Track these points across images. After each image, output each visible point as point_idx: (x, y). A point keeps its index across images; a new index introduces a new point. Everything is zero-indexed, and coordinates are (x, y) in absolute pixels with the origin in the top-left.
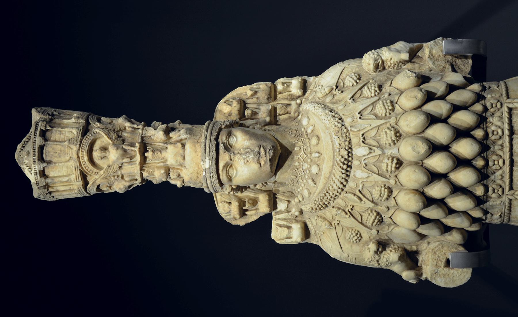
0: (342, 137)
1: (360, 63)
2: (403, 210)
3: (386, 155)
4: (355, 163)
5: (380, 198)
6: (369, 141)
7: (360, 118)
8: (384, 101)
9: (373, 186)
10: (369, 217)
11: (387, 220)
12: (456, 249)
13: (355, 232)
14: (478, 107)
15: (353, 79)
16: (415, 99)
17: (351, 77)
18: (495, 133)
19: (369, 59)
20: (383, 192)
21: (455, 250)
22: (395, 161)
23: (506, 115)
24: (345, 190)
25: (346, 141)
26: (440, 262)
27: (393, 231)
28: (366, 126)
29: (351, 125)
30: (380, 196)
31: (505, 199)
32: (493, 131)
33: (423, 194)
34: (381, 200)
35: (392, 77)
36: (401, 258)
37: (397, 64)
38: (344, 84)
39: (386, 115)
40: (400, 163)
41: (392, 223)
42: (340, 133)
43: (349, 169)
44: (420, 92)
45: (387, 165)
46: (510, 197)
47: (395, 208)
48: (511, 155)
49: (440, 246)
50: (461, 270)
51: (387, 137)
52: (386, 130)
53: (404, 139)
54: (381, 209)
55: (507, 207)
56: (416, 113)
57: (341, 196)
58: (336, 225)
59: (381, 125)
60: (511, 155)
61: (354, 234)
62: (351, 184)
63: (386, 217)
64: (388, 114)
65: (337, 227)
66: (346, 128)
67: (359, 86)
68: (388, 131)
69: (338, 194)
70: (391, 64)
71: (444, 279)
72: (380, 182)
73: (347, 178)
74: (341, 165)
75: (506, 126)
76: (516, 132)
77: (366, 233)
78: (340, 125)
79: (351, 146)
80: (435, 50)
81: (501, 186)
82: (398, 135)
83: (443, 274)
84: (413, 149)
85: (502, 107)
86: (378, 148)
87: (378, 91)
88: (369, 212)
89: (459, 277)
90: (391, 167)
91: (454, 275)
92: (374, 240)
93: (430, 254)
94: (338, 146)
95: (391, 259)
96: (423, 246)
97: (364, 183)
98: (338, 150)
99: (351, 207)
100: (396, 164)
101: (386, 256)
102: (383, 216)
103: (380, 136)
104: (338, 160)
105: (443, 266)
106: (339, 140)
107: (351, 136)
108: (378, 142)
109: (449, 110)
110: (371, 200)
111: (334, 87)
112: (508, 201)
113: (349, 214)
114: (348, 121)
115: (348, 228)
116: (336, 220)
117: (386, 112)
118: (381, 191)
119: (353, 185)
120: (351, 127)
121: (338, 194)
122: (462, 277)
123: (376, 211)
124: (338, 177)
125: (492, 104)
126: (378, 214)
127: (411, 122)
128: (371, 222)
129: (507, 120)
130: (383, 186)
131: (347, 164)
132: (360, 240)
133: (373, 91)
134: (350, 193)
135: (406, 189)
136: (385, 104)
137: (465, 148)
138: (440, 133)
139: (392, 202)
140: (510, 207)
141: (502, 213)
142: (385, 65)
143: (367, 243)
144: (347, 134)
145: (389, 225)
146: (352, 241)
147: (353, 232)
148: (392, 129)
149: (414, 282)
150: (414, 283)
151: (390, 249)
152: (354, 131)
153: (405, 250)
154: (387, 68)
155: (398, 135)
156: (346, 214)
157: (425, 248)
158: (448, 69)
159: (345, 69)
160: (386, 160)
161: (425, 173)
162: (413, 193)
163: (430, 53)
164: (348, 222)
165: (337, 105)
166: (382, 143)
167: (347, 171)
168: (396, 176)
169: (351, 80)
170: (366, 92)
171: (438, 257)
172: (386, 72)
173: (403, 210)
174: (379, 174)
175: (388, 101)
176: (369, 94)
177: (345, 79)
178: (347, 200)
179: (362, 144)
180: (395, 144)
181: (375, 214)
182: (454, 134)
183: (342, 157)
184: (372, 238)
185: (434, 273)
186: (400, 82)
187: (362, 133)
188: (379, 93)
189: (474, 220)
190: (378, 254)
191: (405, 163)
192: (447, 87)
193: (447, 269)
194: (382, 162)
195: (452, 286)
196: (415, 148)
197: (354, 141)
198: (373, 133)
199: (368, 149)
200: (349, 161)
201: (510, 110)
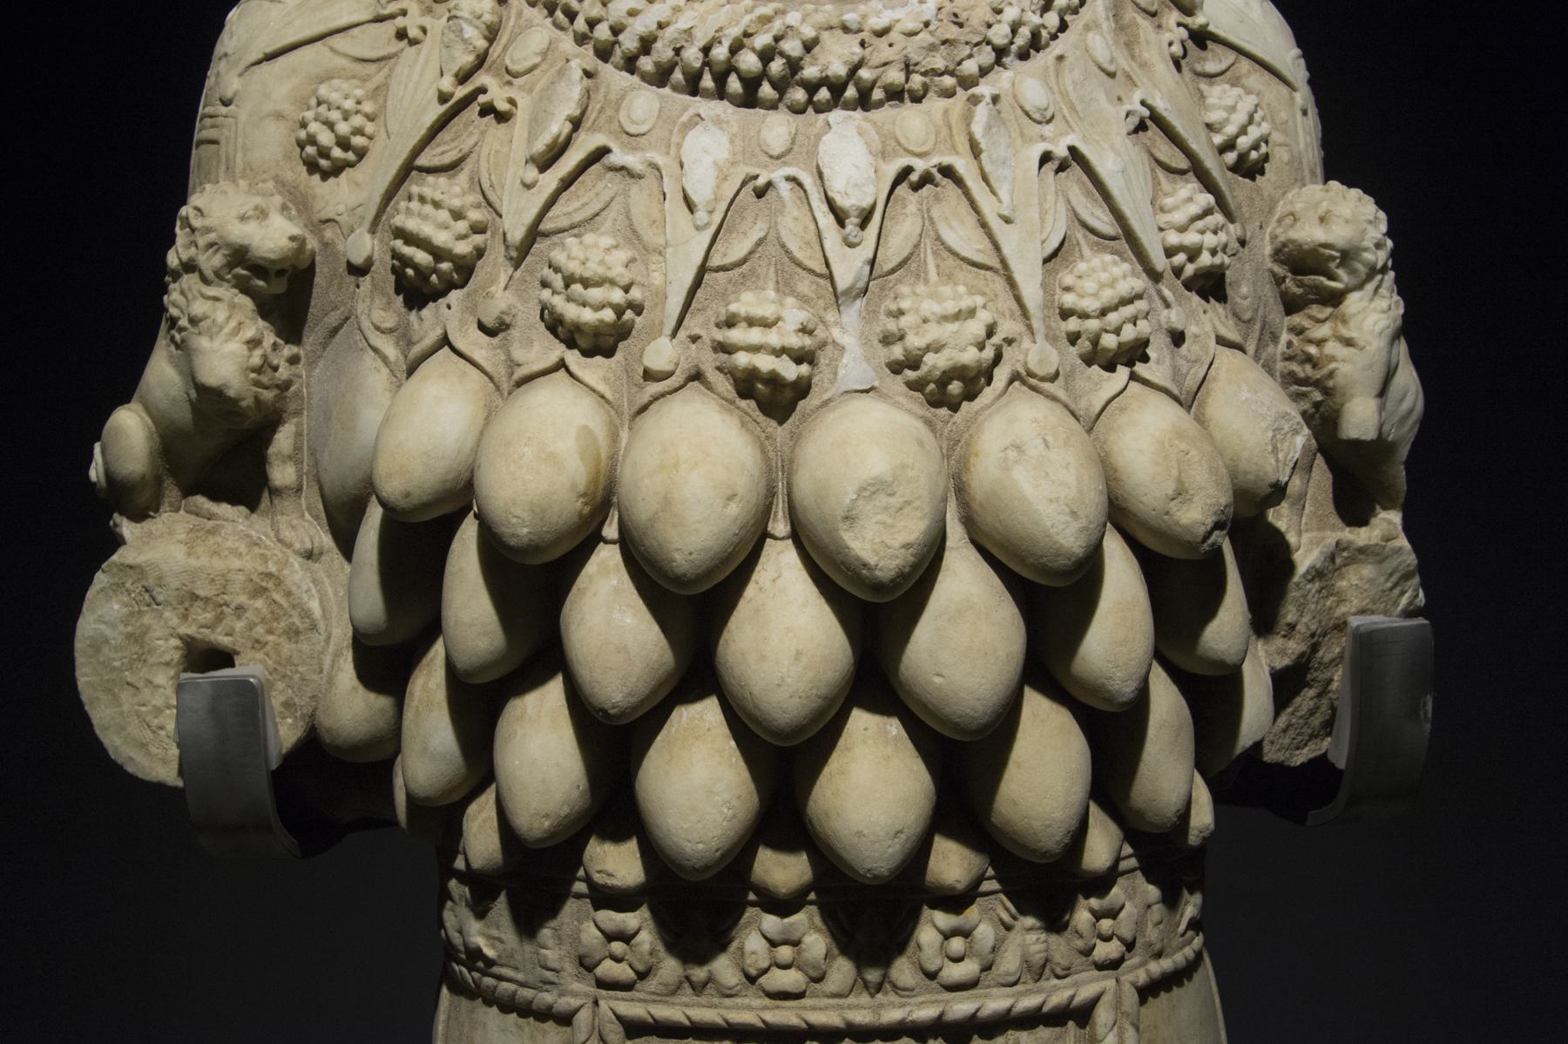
0: (932, 48)
1: (1313, 173)
2: (488, 419)
3: (831, 316)
4: (776, 127)
5: (558, 281)
6: (912, 208)
7: (1046, 158)
8: (1141, 305)
9: (632, 235)
10: (443, 215)
11: (429, 322)
12: (288, 705)
13: (359, 131)
14: (1101, 846)
15: (1243, 131)
16: (1169, 488)
17: (1251, 121)
18: (957, 944)
19: (1350, 218)
20: (595, 294)
21: (276, 700)
22: (790, 371)
23: (1056, 994)
24: (608, 71)
25: (908, 68)
26: (209, 616)
27: (369, 358)
28: (1003, 193)
29: (1004, 105)
30: (569, 281)
32: (966, 933)
33: (584, 541)
34: (545, 284)
35: (1251, 348)
36: (208, 399)
37: (1318, 375)
38: (1211, 77)
39: (1065, 314)
40: (775, 399)
41: (416, 350)
42: (952, 32)
43: (734, 85)
44: (1210, 521)
45: (766, 324)
46: (583, 1018)
47: (500, 372)
49: (297, 621)
50: (171, 726)
51: (945, 318)
52: (984, 317)
53: (929, 423)
54: (498, 290)
56: (1093, 505)
57: (567, 43)
58: (400, 22)
59: (1011, 283)
61: (343, 128)
62: (644, 104)
63: (450, 314)
64: (1073, 324)
65: (389, 28)
66: (984, 72)
67: (1210, 162)
68: (976, 328)
69: (580, 24)
70: (1320, 343)
71: (115, 635)
72: (657, 279)
73: (678, 76)
74: (762, 40)
77: (353, 200)
78: (999, 34)
79: (880, 104)
80: (1360, 573)
81: (642, 976)
82: (950, 391)
83: (146, 630)
84: (875, 488)
85: (1100, 967)
86: (872, 262)
87: (1190, 269)
88: (475, 215)
89: (141, 721)
90: (755, 349)
92: (312, 244)
93: (249, 564)
94: (877, 23)
95: (204, 342)
97: (650, 180)
98: (851, 17)
99: (502, 106)
100: (774, 380)
101: (221, 314)
102: (455, 296)
103: (948, 277)
104: (793, 18)
105: (189, 630)
106: (911, 25)
107: (934, 104)
108: (903, 264)
109: (1097, 690)
110: (546, 226)
111: (1198, 20)
112: (565, 1003)
113: (461, 92)
114: (1025, 83)
115: (380, 92)
116: (427, 21)
117: (1084, 316)
118: (600, 283)
119: (638, 114)
120: (995, 99)
121: (580, 24)
122: (135, 729)
123: (480, 253)
124: (683, 23)
125: (1113, 914)
126: (465, 270)
127: (1036, 468)
128: (412, 225)
129: (1028, 1003)
130: (636, 294)
131: (764, 74)
132: (312, 167)
133: (1191, 238)
134: (588, 94)
135: (614, 437)
136: (1128, 311)
137: (873, 787)
138: (965, 639)
139: (542, 350)
140: (526, 1011)
141: (490, 963)
142: (1316, 310)
143: (298, 203)
144: (948, 81)
145: (404, 337)
146: (309, 115)
147: (357, 121)
148: (989, 353)
149: (95, 473)
150: (93, 475)
151: (270, 338)
152: (968, 119)
153: (269, 421)
154: (1297, 319)
155: (950, 391)
156: (463, 77)
157: (287, 534)
159: (1284, 90)
160: (794, 315)
161: (725, 560)
162: (594, 481)
164: (418, 87)
165: (1107, 26)
166: (904, 289)
167: (721, 79)
168: (697, 376)
169: (1240, 118)
170: (1188, 198)
171: (240, 609)
172: (1275, 313)
173: (488, 419)
174: (703, 270)
175: (1144, 327)
176: (1179, 217)
177: (1235, 83)
178: (541, 79)
179: (891, 169)
180: (896, 368)
181: (463, 248)
182: (956, 727)
183: (809, 46)
184: (329, 234)
185: (150, 582)
186: (1245, 394)
187: (963, 165)
188: (1178, 271)
189: (441, 818)
190: (230, 265)
191: (780, 432)
192: (1221, 664)
193: (177, 655)
194: (785, 287)
195: (85, 677)
196: (882, 500)
197: (911, 121)
198: (963, 237)
199: (866, 203)
200: (781, 86)
201: (1081, 1014)
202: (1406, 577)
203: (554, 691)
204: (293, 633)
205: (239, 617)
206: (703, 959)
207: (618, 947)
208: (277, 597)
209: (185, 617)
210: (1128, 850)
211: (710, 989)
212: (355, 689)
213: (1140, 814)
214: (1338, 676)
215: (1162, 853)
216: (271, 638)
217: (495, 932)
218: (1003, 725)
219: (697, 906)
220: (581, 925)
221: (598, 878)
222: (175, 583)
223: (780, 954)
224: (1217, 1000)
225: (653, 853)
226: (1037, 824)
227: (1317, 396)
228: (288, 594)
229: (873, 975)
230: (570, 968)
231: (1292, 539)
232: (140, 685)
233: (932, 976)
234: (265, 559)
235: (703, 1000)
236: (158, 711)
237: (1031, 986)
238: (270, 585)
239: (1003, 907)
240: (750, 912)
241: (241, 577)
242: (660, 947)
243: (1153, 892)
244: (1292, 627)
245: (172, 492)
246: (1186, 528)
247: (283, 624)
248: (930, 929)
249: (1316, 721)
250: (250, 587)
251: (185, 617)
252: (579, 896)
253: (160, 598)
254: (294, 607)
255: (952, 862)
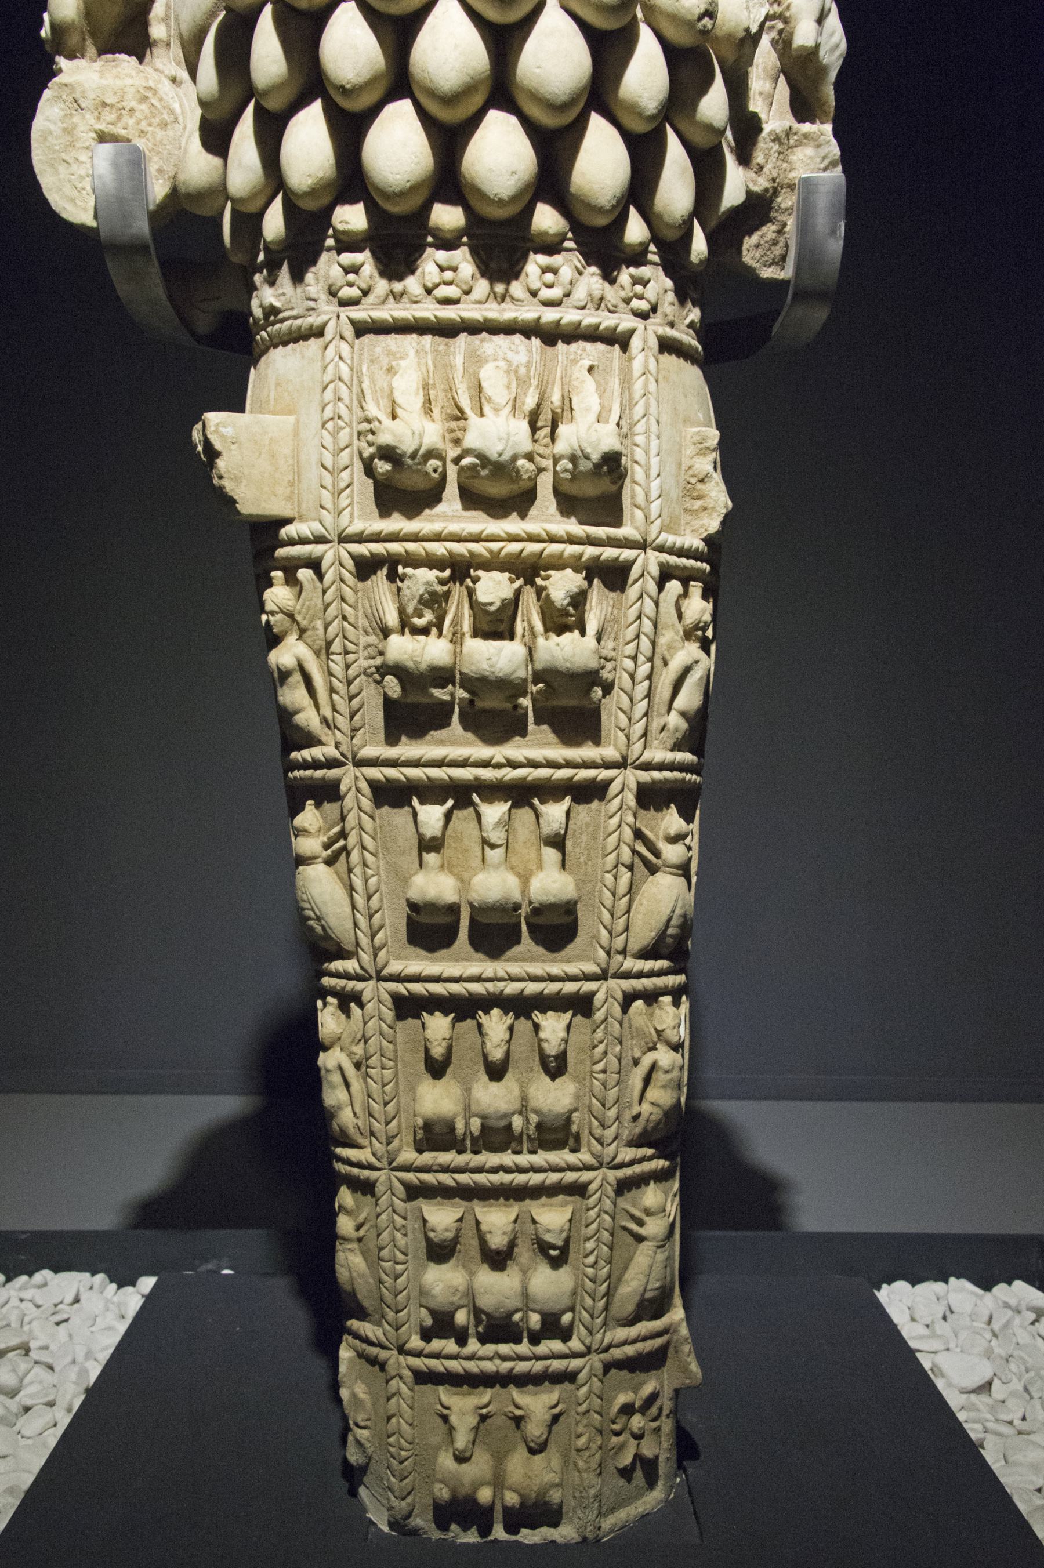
12: (160, 171)
18: (549, 277)
21: (152, 168)
23: (606, 321)
31: (327, 310)
32: (555, 271)
48: (473, 328)
49: (166, 116)
55: (299, 322)
60: (473, 328)
71: (56, 129)
75: (568, 316)
76: (549, 349)
81: (365, 293)
83: (75, 126)
91: (74, 167)
96: (167, 61)
109: (633, 109)
122: (68, 190)
137: (500, 155)
158: (755, 183)
163: (806, 136)
171: (132, 110)
185: (77, 95)
189: (249, 222)
201: (621, 340)
202: (833, 164)
203: (315, 110)
204: (164, 125)
205: (131, 117)
206: (400, 278)
207: (351, 277)
208: (154, 101)
209: (99, 118)
210: (652, 248)
211: (405, 299)
212: (200, 152)
213: (660, 216)
214: (791, 223)
215: (671, 249)
216: (150, 129)
217: (280, 291)
218: (577, 129)
219: (397, 242)
220: (329, 266)
221: (340, 227)
222: (92, 96)
223: (447, 273)
224: (712, 414)
225: (373, 211)
226: (596, 187)
227: (780, 25)
228: (161, 100)
229: (500, 288)
230: (323, 297)
231: (763, 116)
232: (71, 161)
233: (534, 294)
234: (147, 79)
235: (400, 306)
236: (82, 178)
237: (593, 311)
238: (150, 94)
239: (577, 259)
240: (429, 251)
241: (133, 90)
242: (376, 274)
243: (669, 283)
244: (761, 168)
245: (91, 50)
246: (689, 10)
247: (157, 120)
248: (536, 261)
249: (778, 251)
250: (138, 96)
251: (99, 118)
252: (329, 249)
253: (83, 105)
254: (164, 108)
255: (546, 219)
